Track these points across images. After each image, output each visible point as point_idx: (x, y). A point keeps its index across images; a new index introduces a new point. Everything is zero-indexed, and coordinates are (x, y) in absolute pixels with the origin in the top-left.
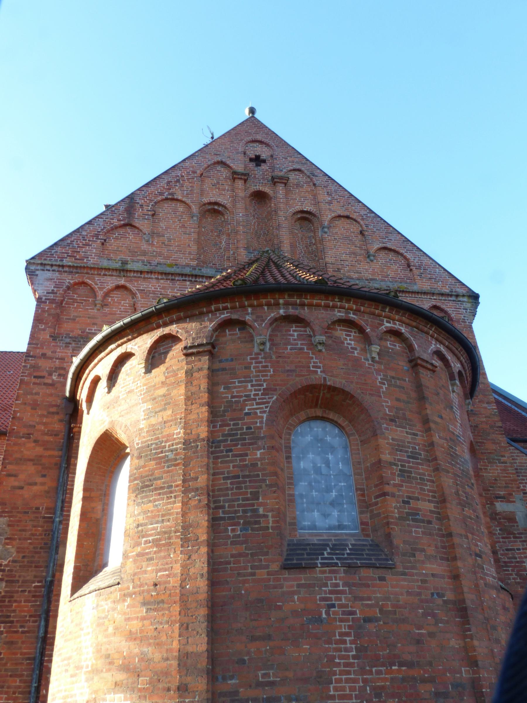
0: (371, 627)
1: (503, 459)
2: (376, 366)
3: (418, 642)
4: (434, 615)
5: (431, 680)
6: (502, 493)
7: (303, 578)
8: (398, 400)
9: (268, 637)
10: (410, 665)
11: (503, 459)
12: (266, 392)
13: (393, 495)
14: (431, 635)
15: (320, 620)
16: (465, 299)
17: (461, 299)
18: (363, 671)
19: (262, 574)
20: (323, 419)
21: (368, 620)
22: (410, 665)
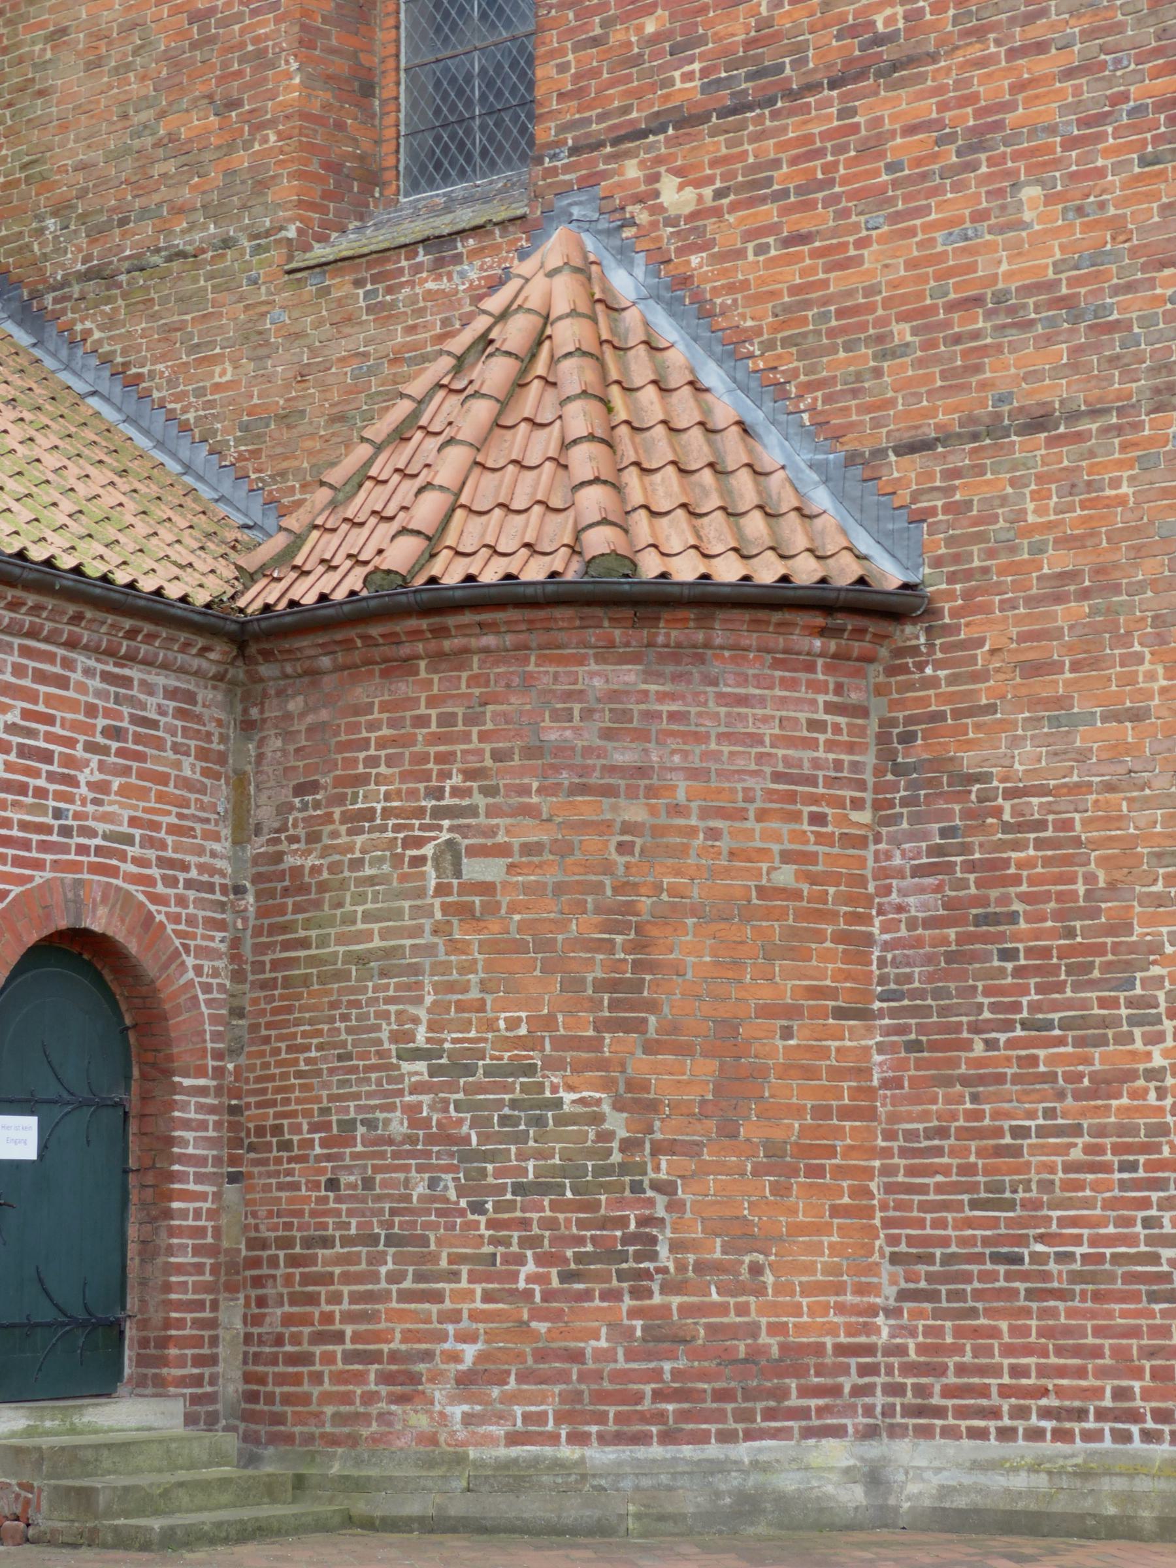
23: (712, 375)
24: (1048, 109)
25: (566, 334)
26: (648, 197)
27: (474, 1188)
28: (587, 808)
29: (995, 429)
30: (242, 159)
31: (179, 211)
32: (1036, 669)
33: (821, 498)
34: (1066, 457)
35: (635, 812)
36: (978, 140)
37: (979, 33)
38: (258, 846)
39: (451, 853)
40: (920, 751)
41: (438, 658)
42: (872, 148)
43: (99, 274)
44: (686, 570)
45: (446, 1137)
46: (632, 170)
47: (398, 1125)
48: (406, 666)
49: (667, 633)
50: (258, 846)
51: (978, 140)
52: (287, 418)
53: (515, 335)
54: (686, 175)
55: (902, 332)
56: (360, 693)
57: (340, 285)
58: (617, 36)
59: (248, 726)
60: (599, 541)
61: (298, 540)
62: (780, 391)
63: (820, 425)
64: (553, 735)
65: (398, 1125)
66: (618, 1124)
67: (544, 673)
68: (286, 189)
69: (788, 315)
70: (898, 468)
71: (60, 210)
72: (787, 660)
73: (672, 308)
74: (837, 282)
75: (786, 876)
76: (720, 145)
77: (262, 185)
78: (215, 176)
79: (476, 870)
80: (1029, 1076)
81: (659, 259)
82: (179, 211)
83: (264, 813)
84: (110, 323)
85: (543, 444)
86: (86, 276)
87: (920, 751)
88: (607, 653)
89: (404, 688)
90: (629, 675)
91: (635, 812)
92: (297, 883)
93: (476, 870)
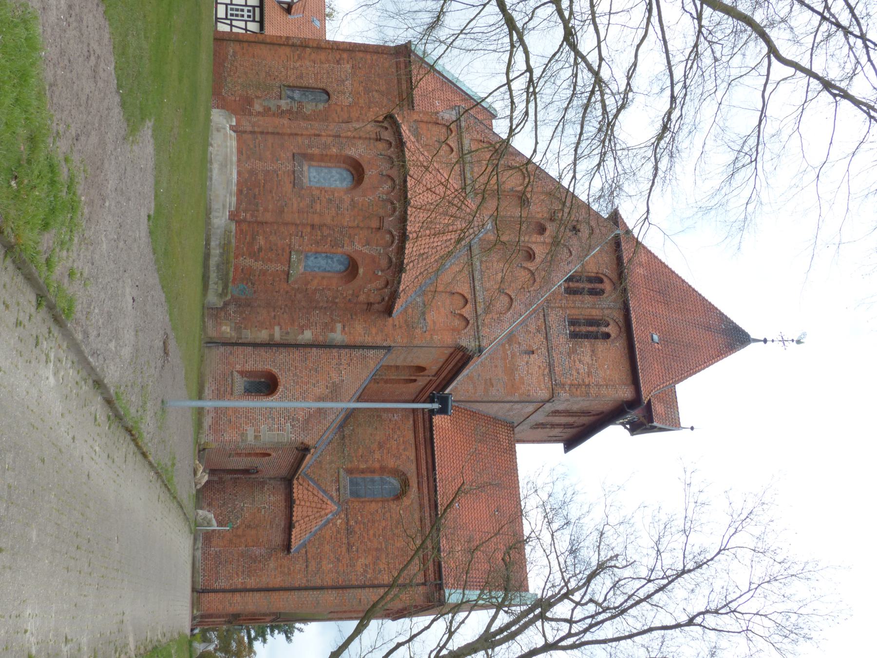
0: (275, 175)
1: (366, 336)
2: (377, 198)
3: (271, 192)
4: (279, 201)
5: (259, 194)
6: (346, 329)
7: (291, 158)
8: (362, 205)
9: (272, 147)
10: (264, 186)
11: (366, 336)
12: (360, 155)
13: (321, 193)
14: (273, 197)
15: (277, 160)
16: (477, 343)
17: (477, 341)
18: (262, 171)
19: (292, 147)
20: (352, 174)
21: (277, 175)
22: (264, 186)
23: (317, 527)
24: (340, 568)
25: (323, 513)
26: (339, 518)
27: (230, 512)
28: (269, 522)
29: (307, 561)
30: (355, 459)
31: (350, 449)
32: (281, 566)
33: (302, 541)
34: (303, 570)
35: (268, 527)
36: (338, 559)
37: (350, 559)
38: (268, 481)
39: (265, 508)
40: (273, 553)
41: (286, 506)
42: (340, 547)
43: (344, 437)
44: (293, 533)
45: (235, 509)
46: (343, 516)
47: (236, 503)
48: (286, 502)
49: (287, 530)
50: (268, 481)
51: (338, 559)
52: (321, 468)
53: (324, 506)
54: (341, 523)
55: (319, 550)
56: (283, 495)
57: (336, 475)
58: (359, 513)
59: (281, 479)
60: (297, 524)
61: (301, 485)
62: (315, 535)
63: (310, 540)
64: (277, 519)
65: (236, 503)
66: (235, 526)
67: (283, 517)
68: (350, 466)
69: (323, 537)
70: (304, 550)
71: (353, 430)
72: (284, 541)
73: (326, 522)
74: (326, 542)
75: (261, 540)
76: (343, 528)
77: (351, 462)
78: (353, 455)
79: (263, 511)
80: (239, 565)
81: (332, 520)
82: (350, 449)
83: (272, 481)
84: (337, 440)
85: (310, 513)
86: (344, 435)
87: (273, 553)
88: (285, 524)
89: (283, 501)
90: (283, 526)
91: (268, 527)
92: (263, 487)
93: (263, 510)
